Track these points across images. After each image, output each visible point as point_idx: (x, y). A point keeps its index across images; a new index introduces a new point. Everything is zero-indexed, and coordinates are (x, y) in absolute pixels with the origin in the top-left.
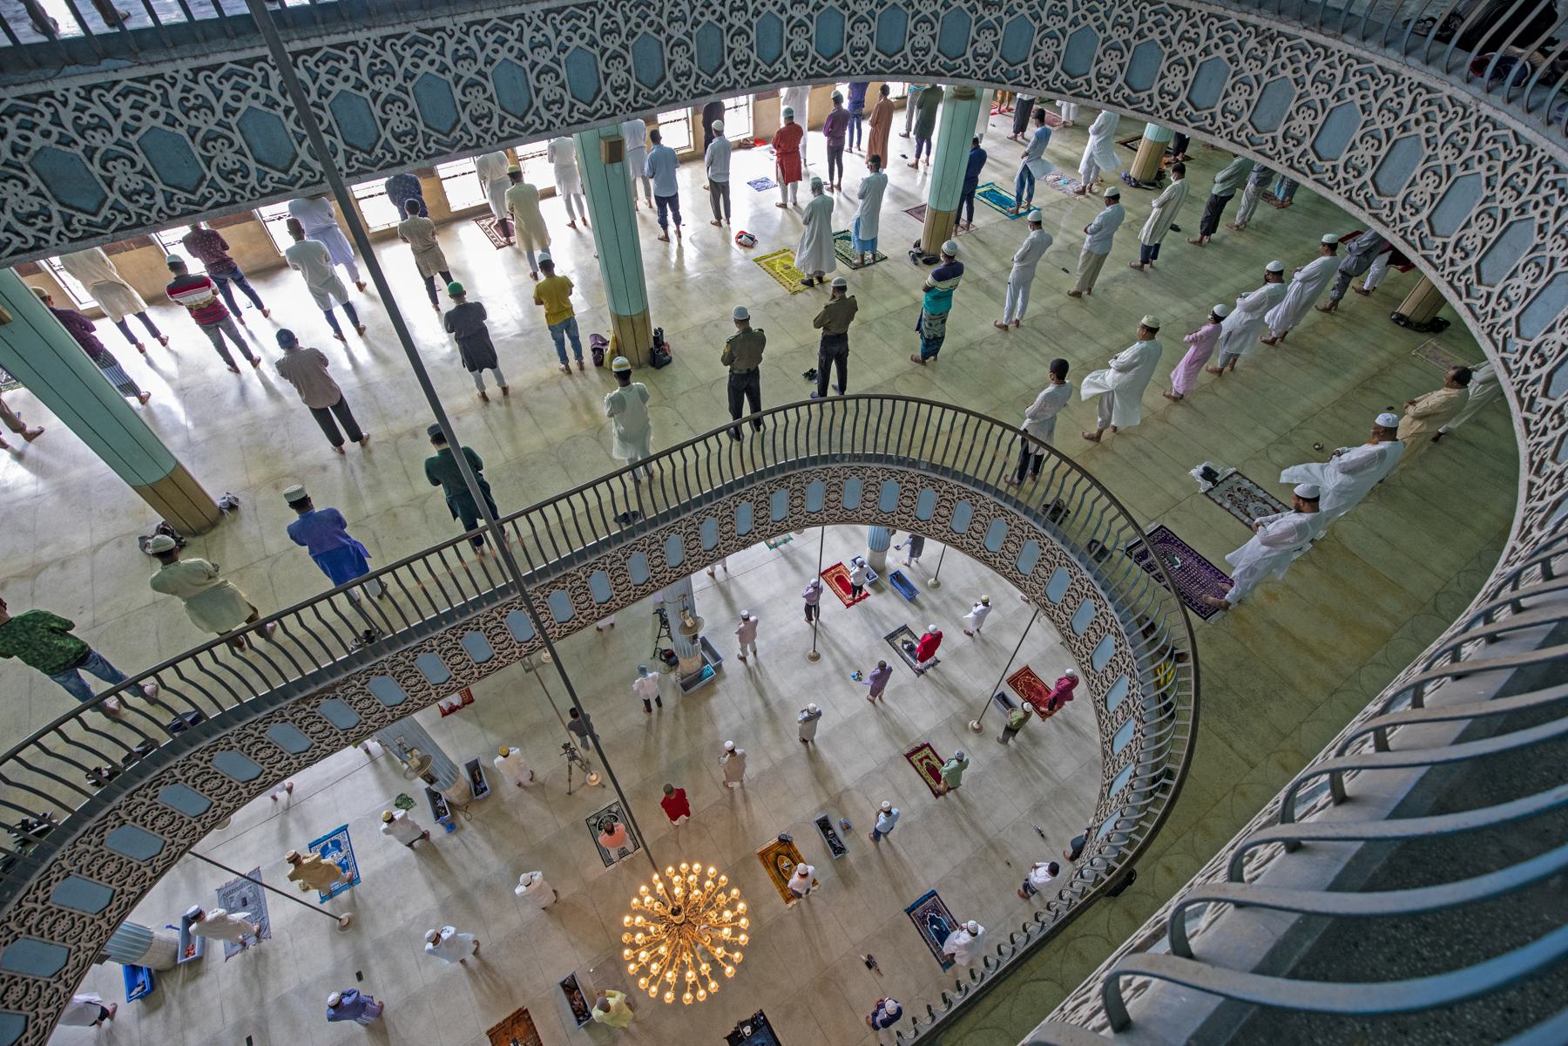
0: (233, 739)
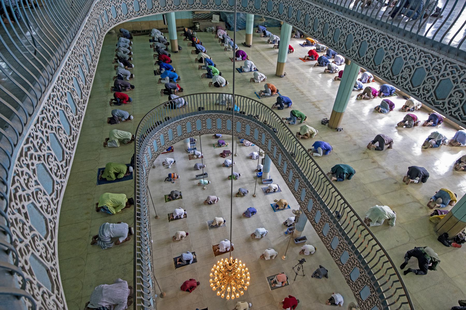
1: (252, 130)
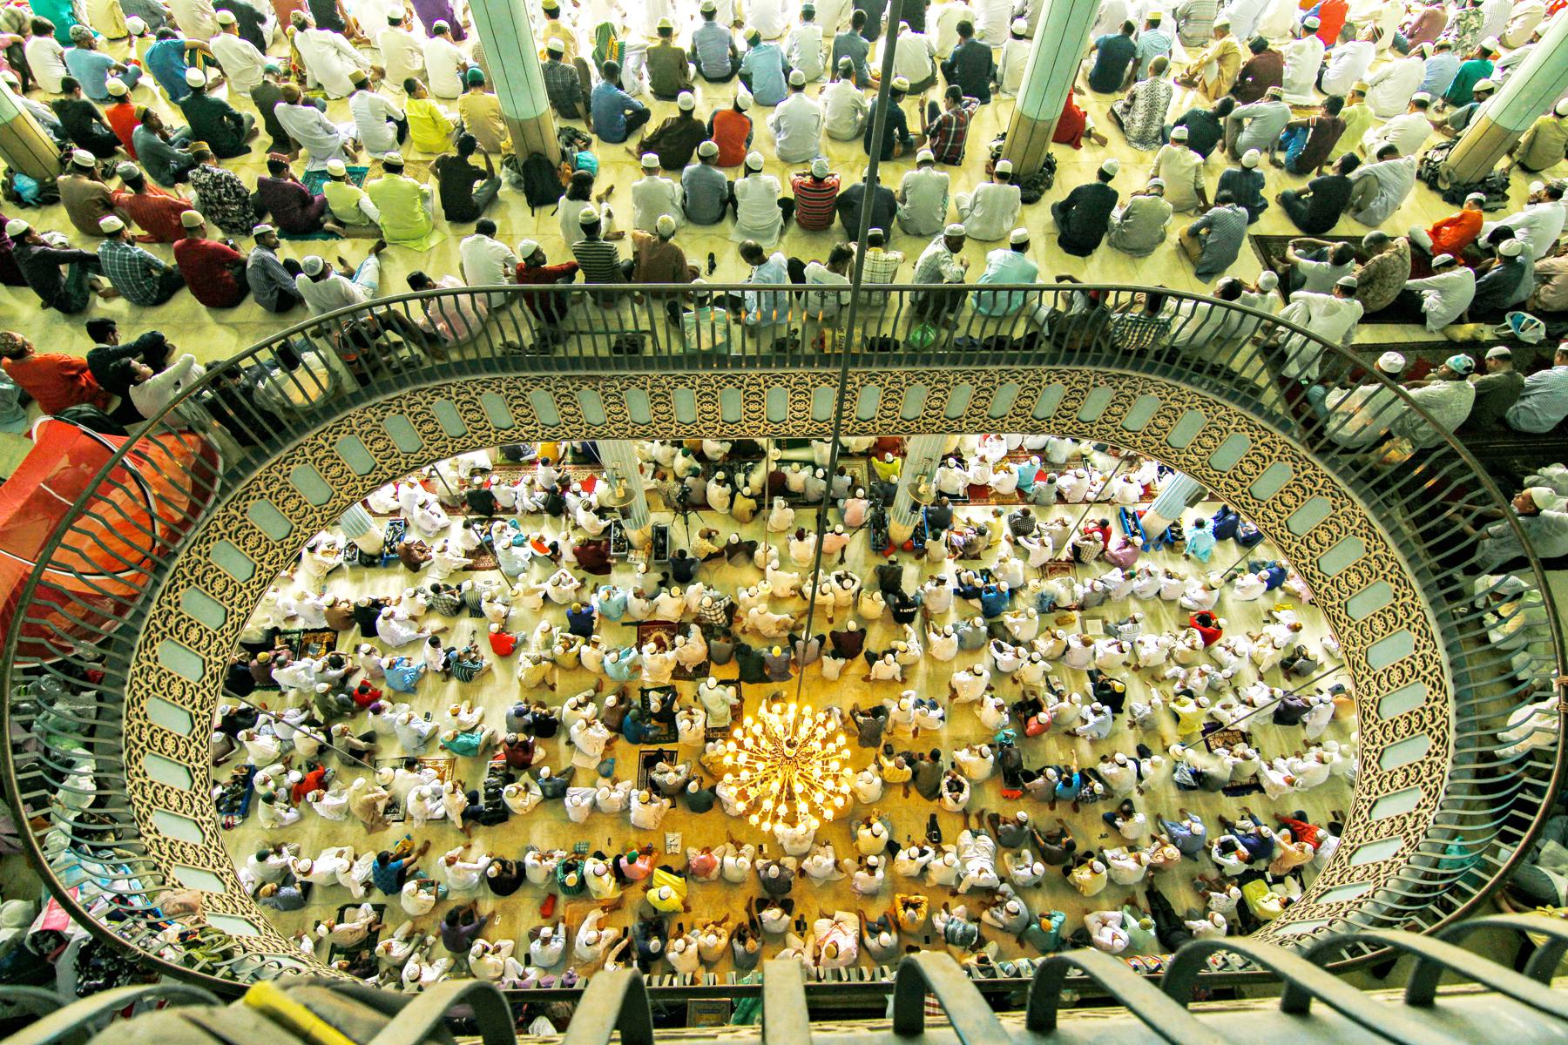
0: (504, 384)
1: (374, 435)
